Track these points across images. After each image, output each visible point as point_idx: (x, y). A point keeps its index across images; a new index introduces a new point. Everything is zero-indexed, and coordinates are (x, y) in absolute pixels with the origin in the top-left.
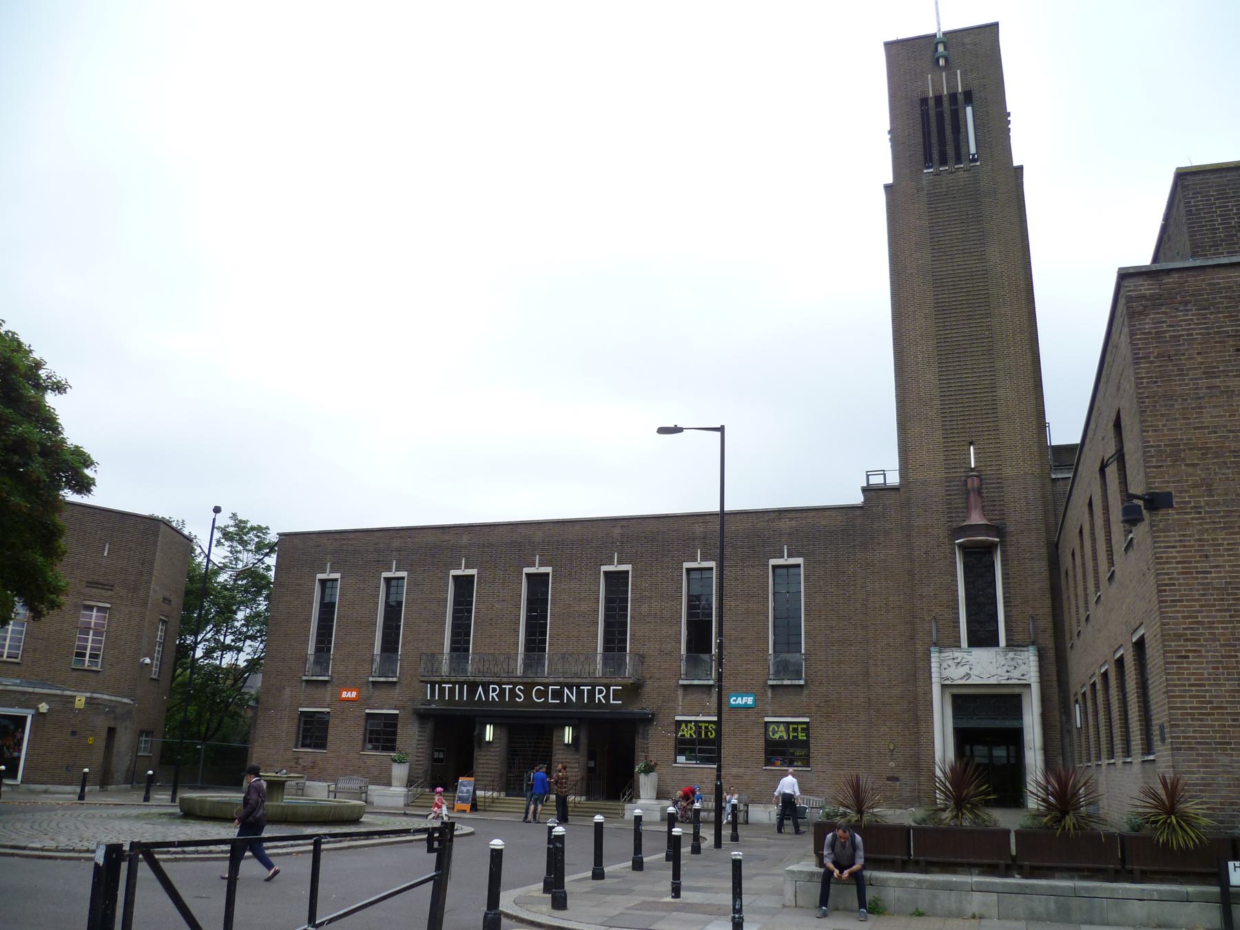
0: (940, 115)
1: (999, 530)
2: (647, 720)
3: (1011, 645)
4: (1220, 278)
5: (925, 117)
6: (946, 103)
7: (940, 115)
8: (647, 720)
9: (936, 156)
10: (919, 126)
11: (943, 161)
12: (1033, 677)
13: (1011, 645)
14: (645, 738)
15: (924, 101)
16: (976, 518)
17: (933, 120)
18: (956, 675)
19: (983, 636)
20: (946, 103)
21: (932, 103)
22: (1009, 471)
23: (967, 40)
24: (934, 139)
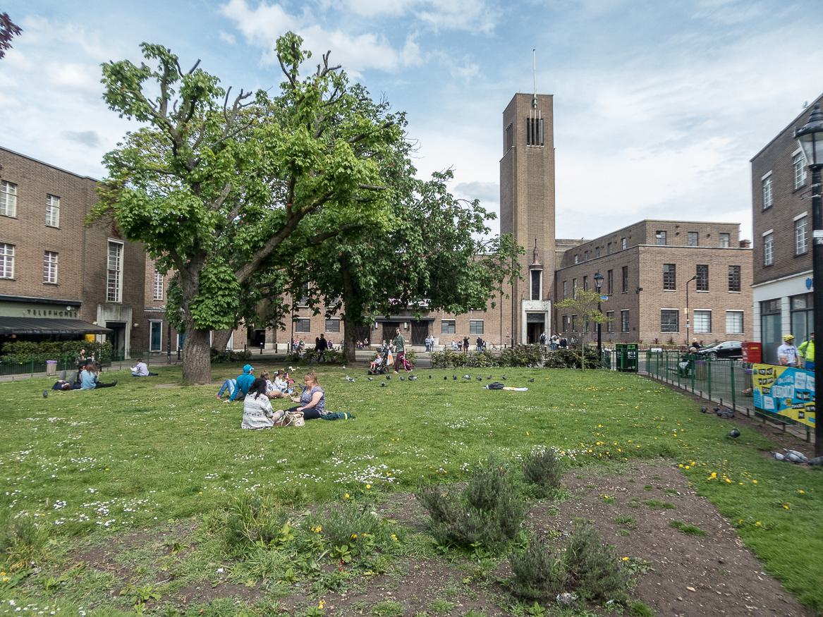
0: (533, 125)
1: (542, 267)
2: (433, 320)
3: (543, 300)
4: (655, 249)
5: (528, 124)
6: (535, 122)
7: (533, 125)
8: (433, 320)
9: (531, 141)
10: (526, 131)
11: (533, 143)
12: (549, 309)
13: (543, 300)
14: (432, 325)
15: (528, 119)
16: (537, 263)
17: (530, 125)
18: (529, 308)
19: (536, 297)
20: (535, 122)
21: (531, 120)
22: (545, 249)
23: (543, 99)
24: (531, 135)
